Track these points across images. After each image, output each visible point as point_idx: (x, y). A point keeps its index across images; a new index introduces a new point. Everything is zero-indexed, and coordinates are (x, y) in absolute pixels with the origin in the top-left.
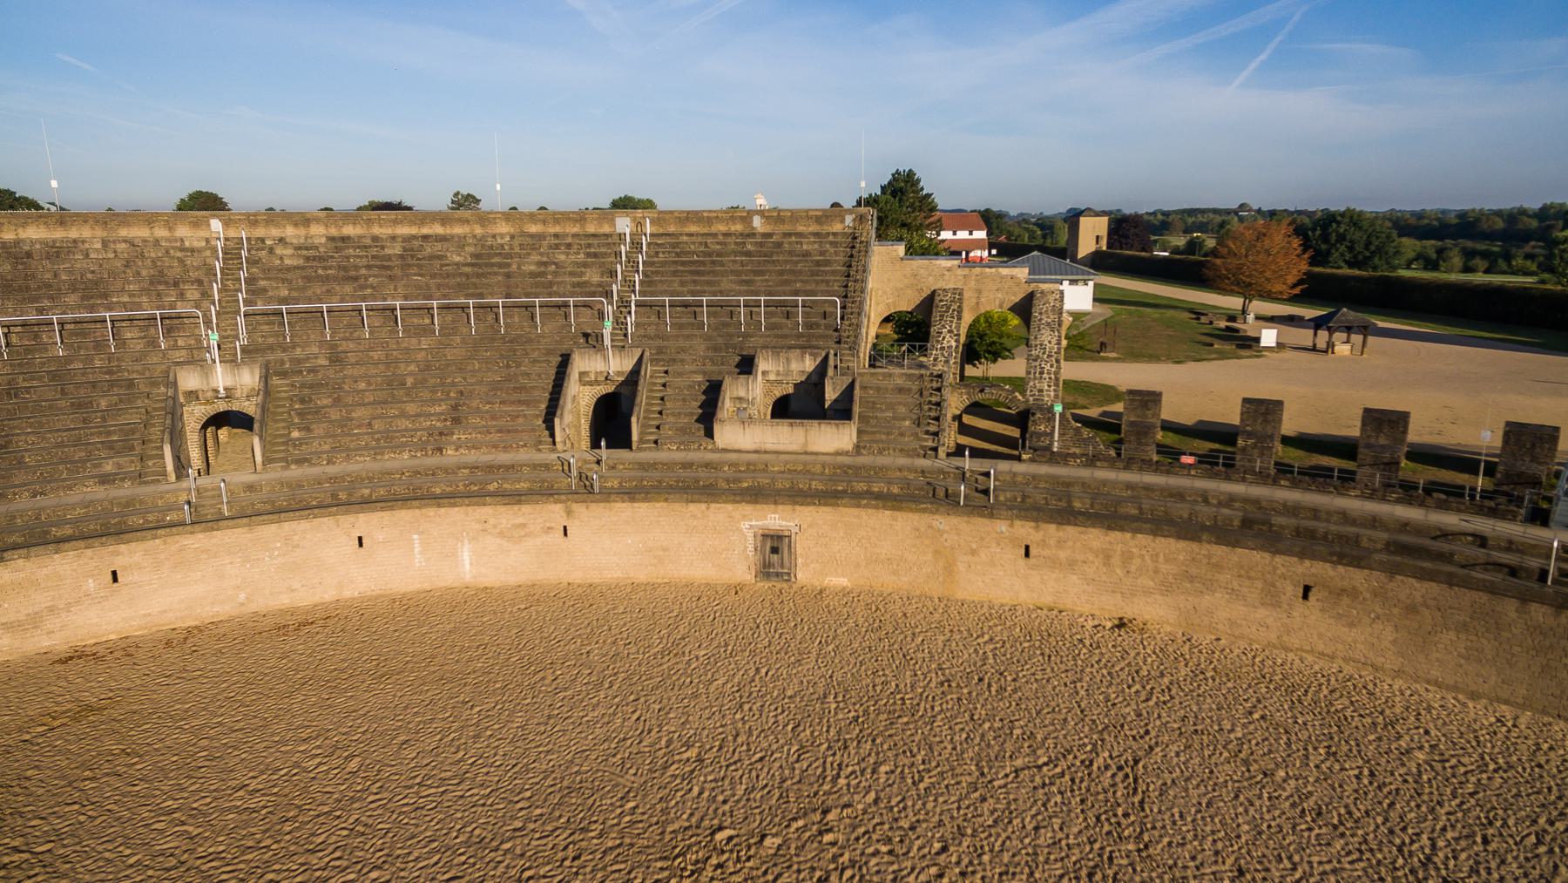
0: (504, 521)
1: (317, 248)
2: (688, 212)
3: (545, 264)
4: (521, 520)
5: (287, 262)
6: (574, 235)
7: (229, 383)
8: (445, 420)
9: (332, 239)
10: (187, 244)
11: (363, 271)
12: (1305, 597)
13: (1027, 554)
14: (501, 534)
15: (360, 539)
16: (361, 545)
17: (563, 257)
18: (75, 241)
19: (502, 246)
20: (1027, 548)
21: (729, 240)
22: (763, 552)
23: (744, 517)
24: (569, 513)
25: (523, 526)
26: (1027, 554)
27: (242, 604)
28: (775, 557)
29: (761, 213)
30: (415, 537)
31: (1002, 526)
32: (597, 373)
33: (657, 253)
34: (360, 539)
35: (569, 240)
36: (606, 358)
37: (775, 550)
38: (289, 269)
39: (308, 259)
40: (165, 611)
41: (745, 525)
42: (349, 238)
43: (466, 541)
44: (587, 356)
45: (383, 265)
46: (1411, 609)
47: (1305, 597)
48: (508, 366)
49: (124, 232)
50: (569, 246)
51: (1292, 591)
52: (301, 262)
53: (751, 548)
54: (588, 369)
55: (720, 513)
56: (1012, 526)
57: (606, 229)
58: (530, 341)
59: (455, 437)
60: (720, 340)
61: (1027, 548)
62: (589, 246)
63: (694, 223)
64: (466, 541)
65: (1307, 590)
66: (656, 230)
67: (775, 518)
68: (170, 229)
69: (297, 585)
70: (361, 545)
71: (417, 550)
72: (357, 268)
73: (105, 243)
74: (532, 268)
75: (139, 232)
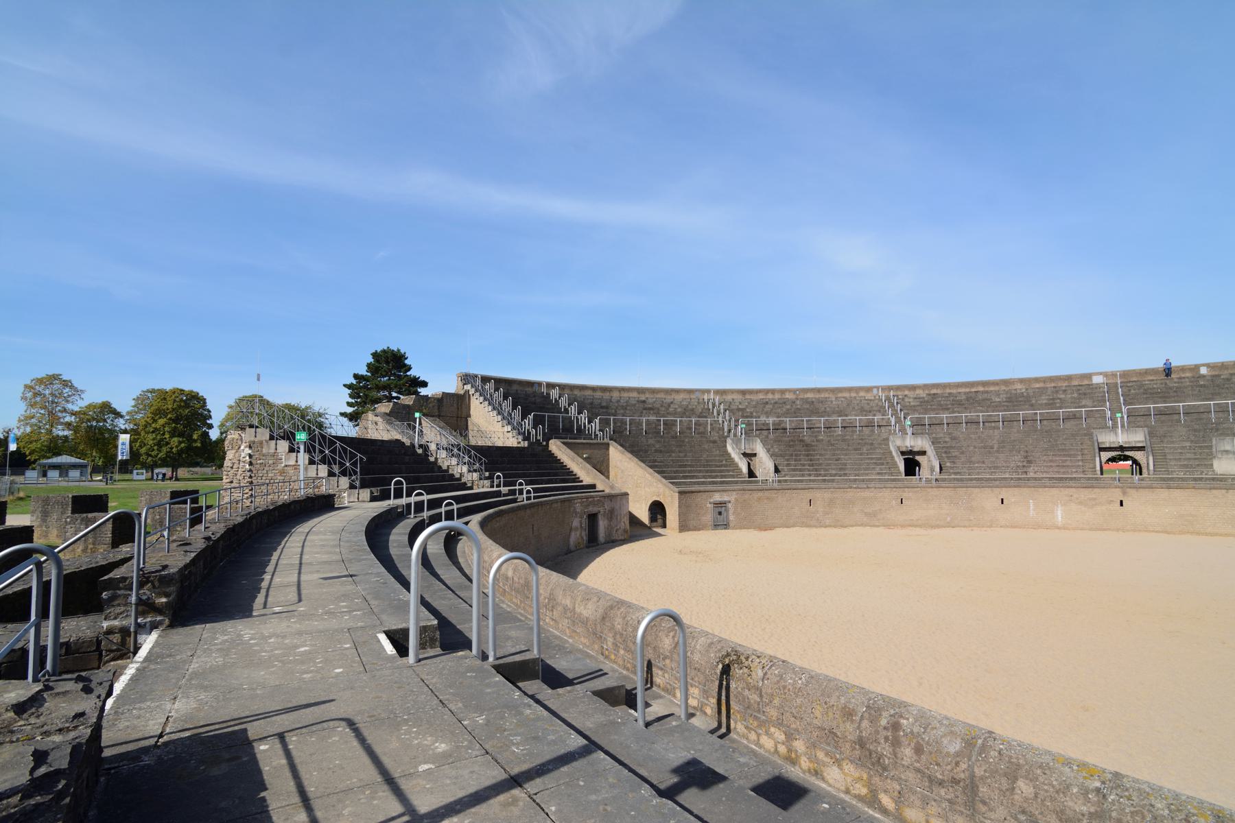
0: (1083, 496)
1: (923, 398)
2: (1147, 370)
3: (1053, 399)
4: (1094, 496)
5: (912, 404)
6: (1066, 386)
7: (912, 444)
8: (1023, 461)
9: (929, 395)
10: (866, 398)
11: (950, 406)
14: (1081, 503)
15: (1002, 500)
16: (1002, 503)
17: (1062, 396)
18: (826, 398)
19: (1022, 393)
21: (1183, 380)
24: (1124, 493)
25: (1095, 499)
27: (948, 523)
30: (1031, 501)
32: (1110, 442)
33: (1130, 390)
34: (1002, 500)
35: (1064, 388)
36: (1116, 434)
38: (914, 406)
39: (921, 402)
40: (918, 520)
42: (937, 394)
43: (1059, 506)
44: (1104, 434)
45: (960, 403)
48: (1050, 441)
49: (840, 395)
50: (1065, 391)
52: (918, 404)
54: (1104, 441)
57: (1086, 382)
58: (1058, 431)
59: (1032, 468)
60: (1197, 427)
62: (1079, 390)
63: (1151, 375)
64: (1059, 506)
66: (1123, 380)
68: (857, 393)
69: (972, 518)
70: (1002, 503)
71: (1031, 508)
72: (947, 405)
73: (836, 398)
74: (1044, 402)
75: (846, 395)
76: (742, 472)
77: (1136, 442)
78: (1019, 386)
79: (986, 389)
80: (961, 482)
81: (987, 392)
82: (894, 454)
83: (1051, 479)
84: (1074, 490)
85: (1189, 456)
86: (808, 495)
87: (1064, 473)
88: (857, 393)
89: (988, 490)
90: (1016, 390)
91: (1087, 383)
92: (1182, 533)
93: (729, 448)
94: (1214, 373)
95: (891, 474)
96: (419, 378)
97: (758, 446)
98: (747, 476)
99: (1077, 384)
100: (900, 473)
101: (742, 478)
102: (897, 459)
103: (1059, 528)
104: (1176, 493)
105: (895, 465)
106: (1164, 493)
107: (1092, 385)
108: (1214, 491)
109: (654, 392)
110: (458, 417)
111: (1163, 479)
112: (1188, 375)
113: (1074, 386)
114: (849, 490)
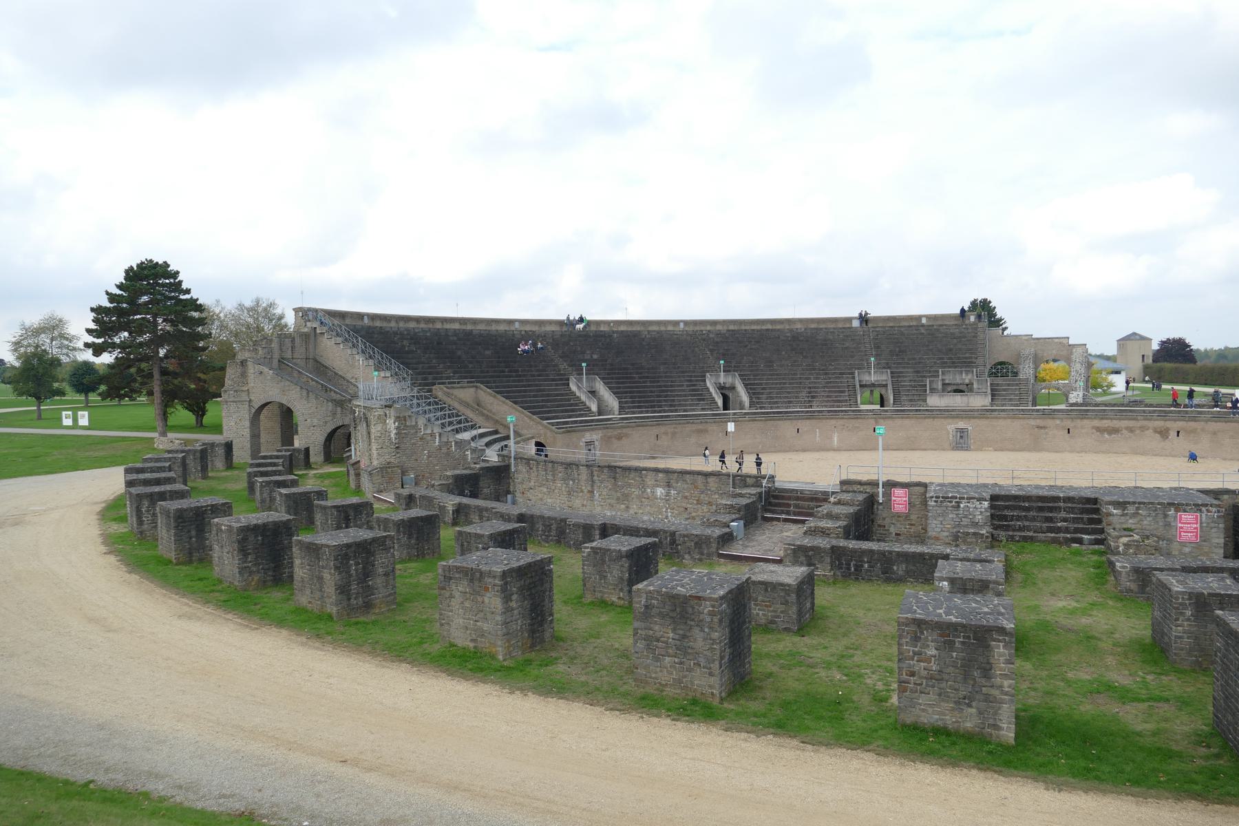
12: (1178, 436)
13: (1069, 433)
20: (1069, 430)
22: (956, 438)
23: (949, 424)
26: (1069, 433)
28: (962, 441)
29: (927, 317)
31: (1058, 422)
37: (961, 437)
41: (949, 427)
46: (1215, 433)
47: (1178, 436)
51: (1173, 434)
53: (951, 436)
55: (938, 423)
56: (1062, 421)
57: (848, 326)
61: (1069, 430)
65: (1178, 432)
67: (961, 424)
68: (666, 327)
76: (590, 410)
77: (883, 381)
78: (799, 326)
79: (774, 328)
80: (769, 417)
81: (775, 330)
82: (712, 390)
83: (829, 411)
84: (845, 420)
85: (914, 392)
86: (655, 430)
87: (838, 407)
88: (666, 327)
89: (788, 422)
90: (797, 329)
91: (849, 326)
92: (907, 450)
93: (573, 387)
94: (930, 324)
95: (711, 409)
96: (197, 299)
97: (597, 384)
98: (597, 414)
99: (841, 326)
100: (719, 408)
101: (592, 416)
102: (714, 395)
103: (834, 450)
104: (907, 422)
105: (714, 402)
106: (899, 422)
107: (852, 327)
108: (927, 420)
109: (475, 323)
110: (306, 359)
111: (898, 411)
112: (914, 323)
113: (841, 328)
114: (687, 425)
